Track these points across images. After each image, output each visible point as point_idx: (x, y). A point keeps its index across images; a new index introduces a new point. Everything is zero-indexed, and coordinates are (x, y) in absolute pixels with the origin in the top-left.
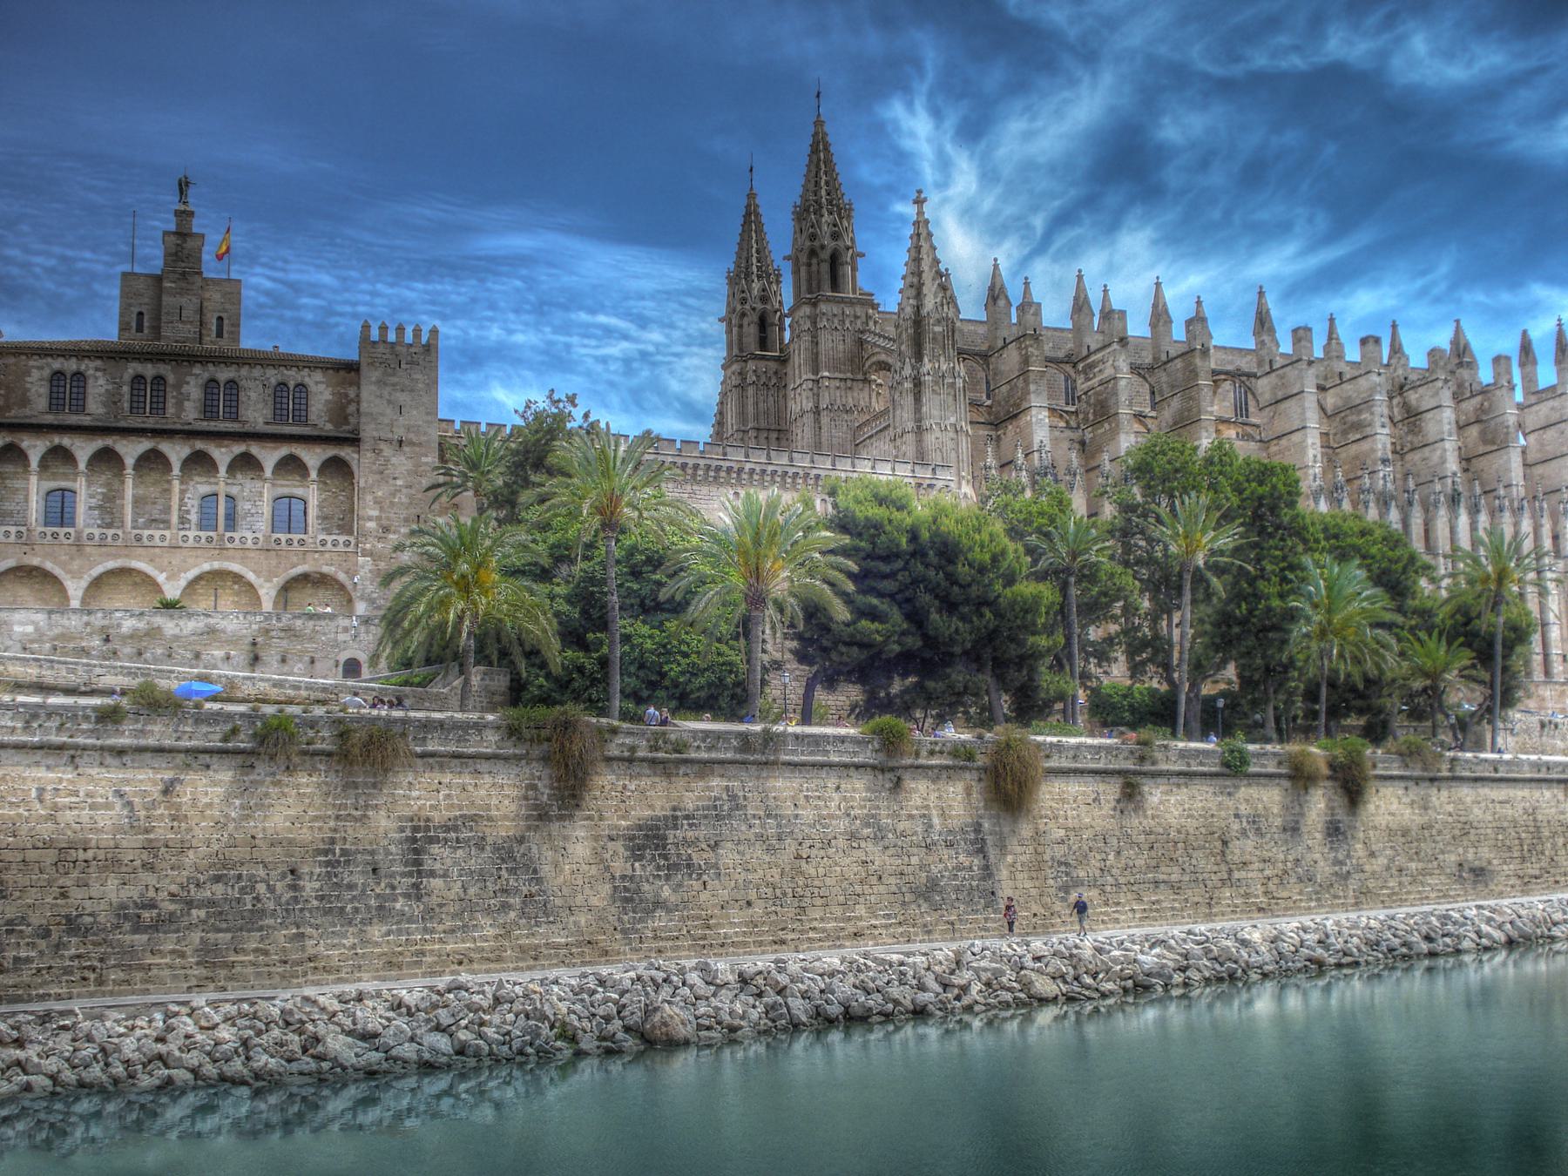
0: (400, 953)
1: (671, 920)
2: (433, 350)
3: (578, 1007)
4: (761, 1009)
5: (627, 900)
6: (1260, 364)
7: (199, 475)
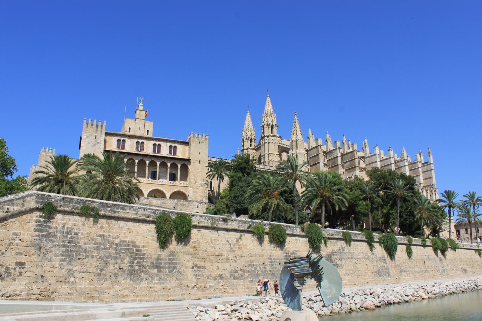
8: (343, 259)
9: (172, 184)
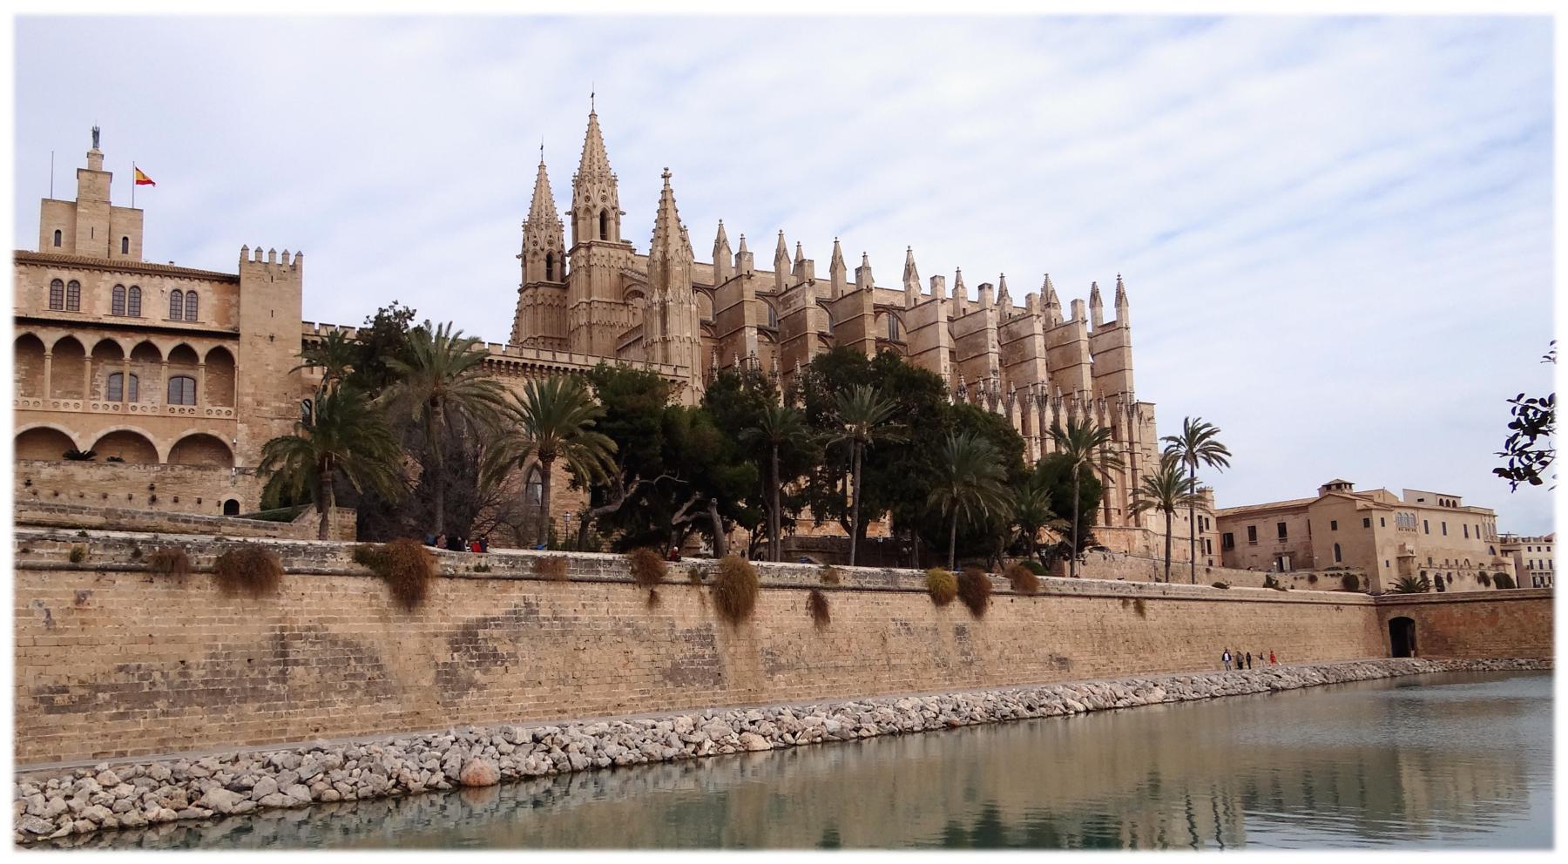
0: (269, 724)
1: (480, 696)
2: (298, 271)
3: (409, 763)
4: (549, 761)
5: (448, 681)
6: (908, 300)
7: (108, 358)
8: (525, 640)
9: (177, 414)
